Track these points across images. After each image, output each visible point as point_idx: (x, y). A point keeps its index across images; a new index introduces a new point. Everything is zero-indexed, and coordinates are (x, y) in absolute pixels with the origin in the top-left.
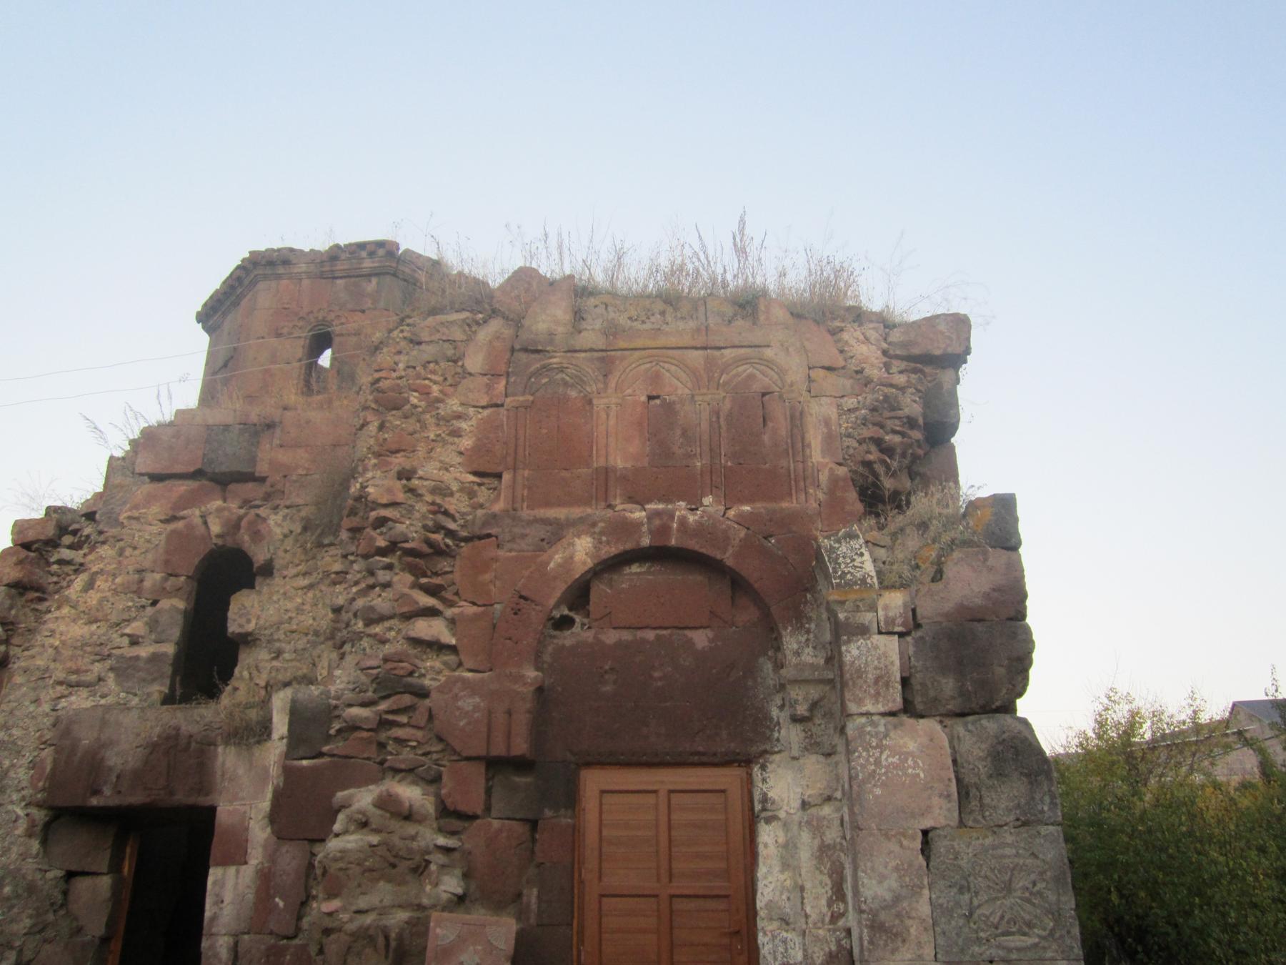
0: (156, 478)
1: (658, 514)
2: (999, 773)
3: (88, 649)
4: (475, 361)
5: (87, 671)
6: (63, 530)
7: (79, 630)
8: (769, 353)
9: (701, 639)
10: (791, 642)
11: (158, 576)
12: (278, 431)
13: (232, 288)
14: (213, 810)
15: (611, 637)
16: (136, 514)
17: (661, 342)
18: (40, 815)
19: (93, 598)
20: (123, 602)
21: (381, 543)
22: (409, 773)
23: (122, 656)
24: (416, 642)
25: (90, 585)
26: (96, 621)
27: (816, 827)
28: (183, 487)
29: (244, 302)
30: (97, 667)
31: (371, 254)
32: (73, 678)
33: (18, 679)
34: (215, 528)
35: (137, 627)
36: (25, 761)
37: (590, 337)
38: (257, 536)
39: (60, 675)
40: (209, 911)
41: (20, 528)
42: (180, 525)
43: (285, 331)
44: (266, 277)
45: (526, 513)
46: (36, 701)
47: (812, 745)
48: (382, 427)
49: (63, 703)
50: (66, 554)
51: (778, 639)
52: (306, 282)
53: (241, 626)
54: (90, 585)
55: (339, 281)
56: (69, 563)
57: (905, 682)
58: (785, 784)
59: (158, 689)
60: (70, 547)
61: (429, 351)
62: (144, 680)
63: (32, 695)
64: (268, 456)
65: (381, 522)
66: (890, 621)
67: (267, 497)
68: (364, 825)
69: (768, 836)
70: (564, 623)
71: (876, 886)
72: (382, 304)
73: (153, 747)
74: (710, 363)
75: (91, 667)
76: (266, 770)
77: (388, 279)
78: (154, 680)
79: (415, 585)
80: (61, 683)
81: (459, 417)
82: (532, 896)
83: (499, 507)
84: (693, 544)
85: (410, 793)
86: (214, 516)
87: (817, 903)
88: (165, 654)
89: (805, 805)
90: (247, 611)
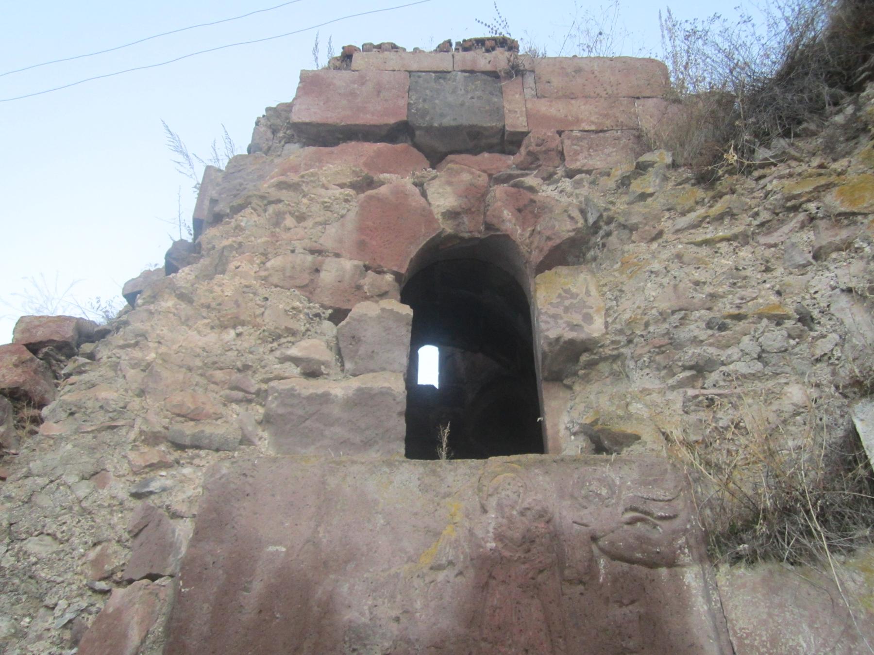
3: (219, 375)
5: (218, 417)
11: (348, 264)
12: (530, 80)
16: (294, 178)
20: (283, 303)
23: (291, 393)
26: (236, 322)
32: (189, 429)
36: (52, 623)
46: (96, 475)
49: (161, 480)
53: (574, 327)
62: (345, 442)
63: (87, 462)
73: (488, 569)
75: (221, 409)
78: (367, 444)
88: (385, 393)
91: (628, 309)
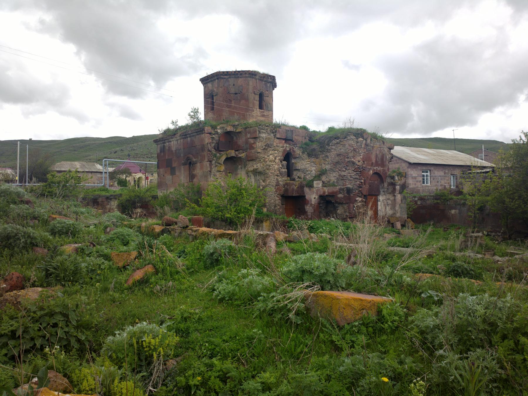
4: (363, 146)
7: (276, 166)
13: (237, 74)
14: (305, 196)
27: (384, 202)
29: (240, 79)
34: (288, 149)
37: (372, 145)
38: (294, 151)
44: (250, 77)
47: (385, 194)
58: (381, 198)
64: (295, 138)
68: (360, 202)
69: (379, 203)
71: (397, 208)
76: (314, 192)
83: (364, 166)
86: (288, 147)
87: (383, 210)
91: (302, 167)
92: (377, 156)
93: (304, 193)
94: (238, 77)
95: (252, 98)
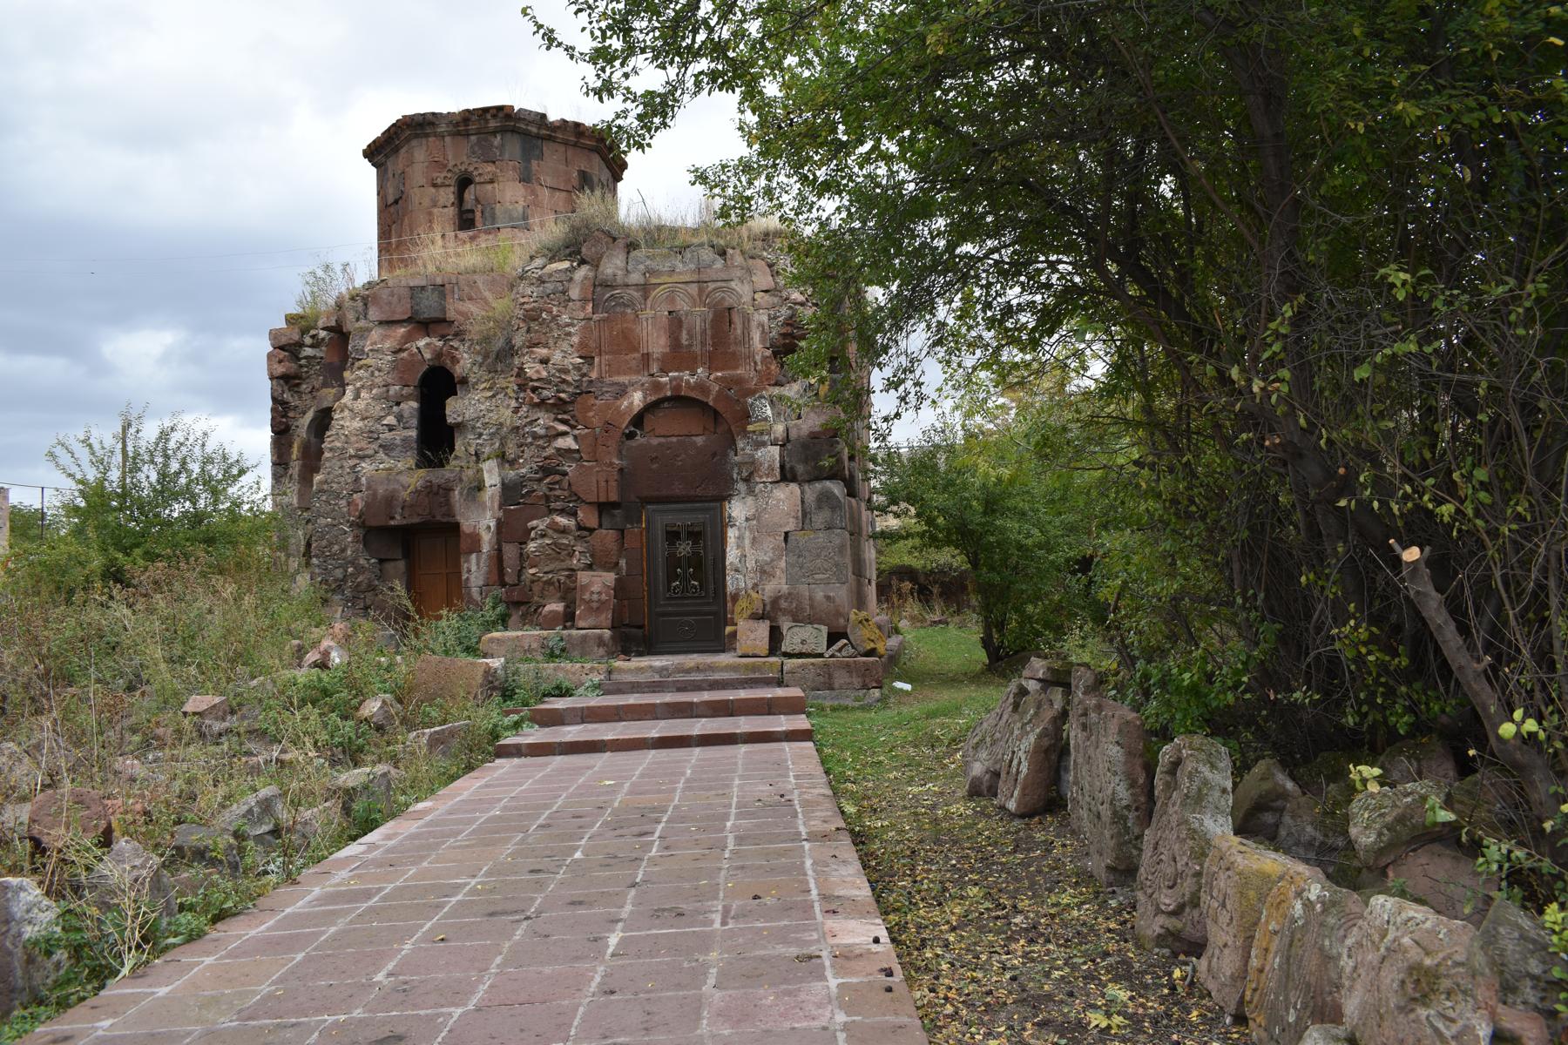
0: (381, 323)
1: (675, 378)
2: (819, 508)
4: (575, 293)
6: (304, 332)
7: (357, 424)
8: (733, 284)
9: (699, 440)
10: (740, 444)
14: (457, 526)
15: (655, 441)
17: (675, 278)
18: (361, 532)
19: (360, 405)
21: (536, 400)
22: (562, 512)
24: (558, 450)
25: (357, 397)
28: (402, 330)
29: (403, 151)
30: (375, 446)
31: (494, 116)
33: (327, 455)
34: (428, 356)
35: (390, 420)
37: (636, 278)
38: (455, 360)
39: (352, 452)
40: (465, 576)
41: (274, 335)
42: (404, 355)
43: (439, 181)
44: (417, 136)
45: (608, 380)
47: (751, 492)
48: (528, 331)
50: (308, 351)
51: (734, 442)
52: (448, 139)
54: (357, 397)
55: (473, 138)
56: (314, 357)
57: (782, 467)
58: (738, 509)
59: (410, 460)
60: (312, 346)
61: (550, 287)
64: (453, 309)
65: (534, 390)
66: (776, 439)
67: (456, 335)
68: (543, 536)
69: (732, 534)
70: (631, 436)
72: (507, 156)
74: (701, 291)
77: (509, 135)
79: (556, 419)
80: (351, 457)
81: (568, 325)
82: (623, 562)
83: (594, 375)
84: (693, 395)
85: (562, 521)
89: (747, 519)
90: (457, 408)
92: (675, 322)
93: (450, 512)
94: (396, 150)
95: (426, 202)
